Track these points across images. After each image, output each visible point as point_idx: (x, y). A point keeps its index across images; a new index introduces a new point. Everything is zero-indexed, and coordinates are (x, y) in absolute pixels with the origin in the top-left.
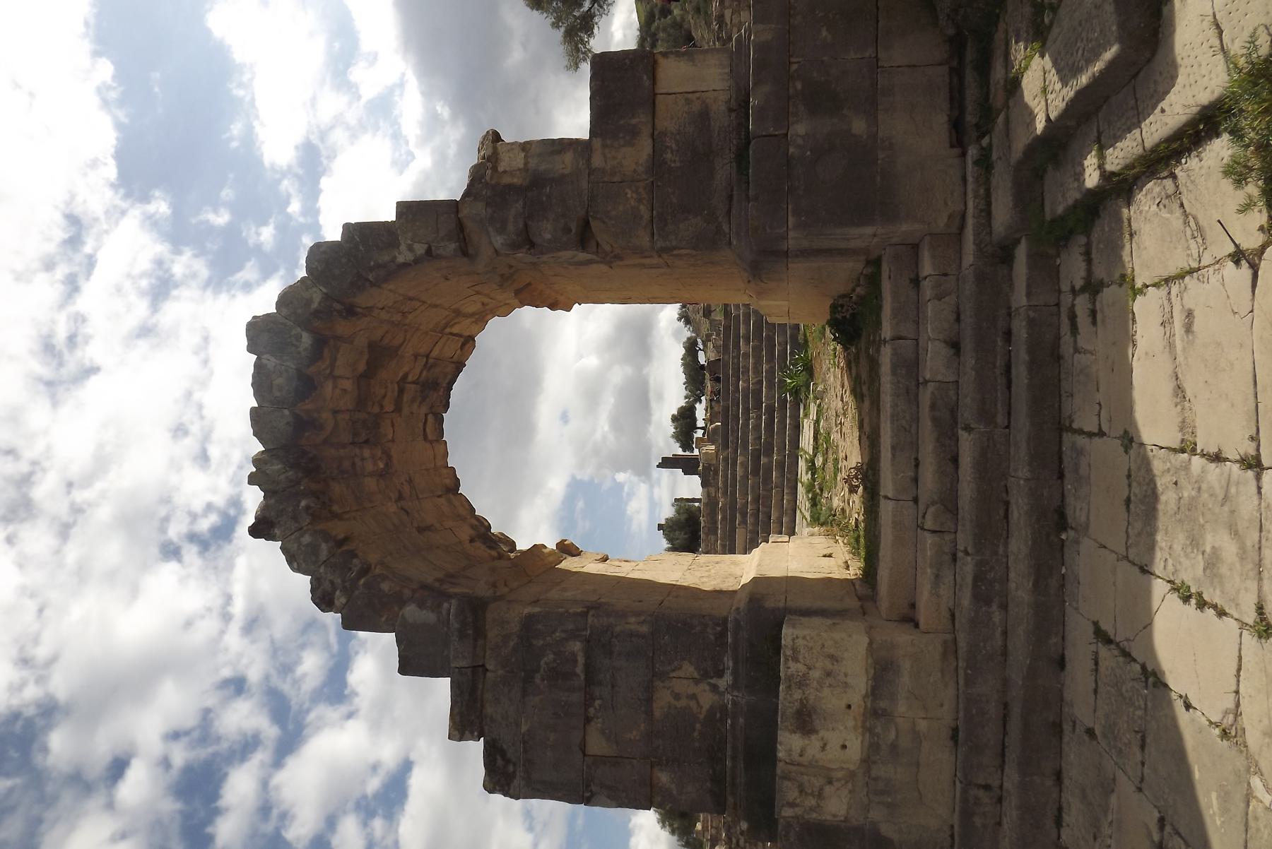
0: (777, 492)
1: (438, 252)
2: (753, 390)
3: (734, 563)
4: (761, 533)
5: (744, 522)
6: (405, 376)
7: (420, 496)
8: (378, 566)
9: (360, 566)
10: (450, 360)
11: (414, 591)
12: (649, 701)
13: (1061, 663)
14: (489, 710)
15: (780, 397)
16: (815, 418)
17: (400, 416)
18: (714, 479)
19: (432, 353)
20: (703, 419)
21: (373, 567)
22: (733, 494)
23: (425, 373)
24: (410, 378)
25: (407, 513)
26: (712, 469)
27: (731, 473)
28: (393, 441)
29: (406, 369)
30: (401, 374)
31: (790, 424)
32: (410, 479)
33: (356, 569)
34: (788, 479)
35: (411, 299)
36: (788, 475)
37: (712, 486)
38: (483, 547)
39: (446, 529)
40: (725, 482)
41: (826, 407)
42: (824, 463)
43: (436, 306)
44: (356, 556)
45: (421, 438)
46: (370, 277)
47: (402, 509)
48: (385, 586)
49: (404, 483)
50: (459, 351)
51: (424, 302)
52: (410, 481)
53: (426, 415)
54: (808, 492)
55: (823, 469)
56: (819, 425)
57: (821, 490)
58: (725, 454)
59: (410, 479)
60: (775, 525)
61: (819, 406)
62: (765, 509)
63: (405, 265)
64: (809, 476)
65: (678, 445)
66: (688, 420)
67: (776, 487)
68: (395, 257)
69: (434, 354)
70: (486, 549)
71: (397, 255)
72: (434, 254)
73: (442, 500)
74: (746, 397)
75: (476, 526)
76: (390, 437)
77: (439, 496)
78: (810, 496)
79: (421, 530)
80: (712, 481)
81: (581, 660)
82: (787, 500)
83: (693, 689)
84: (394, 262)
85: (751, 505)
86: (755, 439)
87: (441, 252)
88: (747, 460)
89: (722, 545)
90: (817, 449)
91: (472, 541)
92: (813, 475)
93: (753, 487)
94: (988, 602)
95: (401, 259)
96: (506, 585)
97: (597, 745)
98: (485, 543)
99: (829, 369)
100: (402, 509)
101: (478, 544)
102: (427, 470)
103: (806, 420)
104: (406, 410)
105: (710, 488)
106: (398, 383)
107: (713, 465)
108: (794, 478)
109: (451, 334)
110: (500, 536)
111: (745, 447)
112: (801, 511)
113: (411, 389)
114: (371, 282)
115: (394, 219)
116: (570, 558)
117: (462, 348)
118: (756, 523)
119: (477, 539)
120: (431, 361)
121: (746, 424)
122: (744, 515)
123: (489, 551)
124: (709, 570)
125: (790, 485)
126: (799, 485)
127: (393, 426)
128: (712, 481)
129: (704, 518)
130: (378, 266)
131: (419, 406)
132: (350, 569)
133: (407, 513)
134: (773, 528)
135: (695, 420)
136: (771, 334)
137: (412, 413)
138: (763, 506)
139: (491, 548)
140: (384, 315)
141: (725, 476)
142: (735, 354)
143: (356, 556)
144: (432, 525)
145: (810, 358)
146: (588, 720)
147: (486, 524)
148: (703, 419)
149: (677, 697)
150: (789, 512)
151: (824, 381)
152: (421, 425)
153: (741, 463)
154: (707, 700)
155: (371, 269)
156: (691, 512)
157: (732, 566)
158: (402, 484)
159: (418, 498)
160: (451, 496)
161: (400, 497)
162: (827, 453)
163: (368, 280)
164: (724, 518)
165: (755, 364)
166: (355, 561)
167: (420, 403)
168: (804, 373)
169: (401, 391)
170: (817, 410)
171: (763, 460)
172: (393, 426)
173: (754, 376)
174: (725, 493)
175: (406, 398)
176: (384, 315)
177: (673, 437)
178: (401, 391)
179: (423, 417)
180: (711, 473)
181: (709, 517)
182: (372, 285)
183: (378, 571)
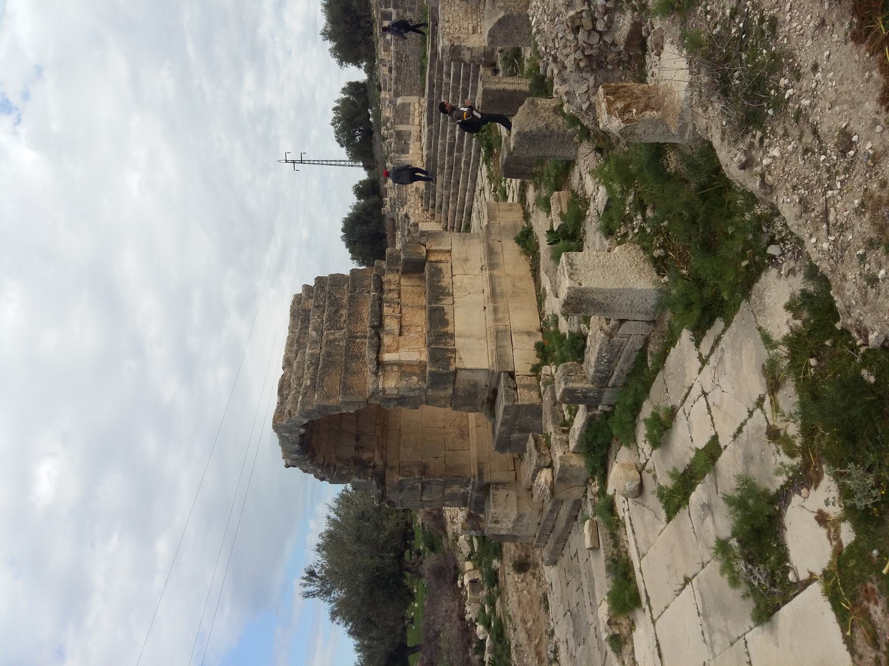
11: (354, 469)
12: (444, 492)
13: (570, 533)
14: (387, 495)
18: (402, 3)
37: (400, 8)
48: (344, 472)
80: (400, 5)
81: (420, 487)
82: (471, 186)
83: (458, 489)
86: (451, 137)
93: (448, 162)
94: (553, 512)
97: (425, 498)
105: (399, 9)
108: (475, 175)
111: (444, 135)
122: (442, 169)
128: (400, 5)
136: (466, 87)
146: (422, 495)
149: (453, 490)
154: (462, 490)
165: (453, 96)
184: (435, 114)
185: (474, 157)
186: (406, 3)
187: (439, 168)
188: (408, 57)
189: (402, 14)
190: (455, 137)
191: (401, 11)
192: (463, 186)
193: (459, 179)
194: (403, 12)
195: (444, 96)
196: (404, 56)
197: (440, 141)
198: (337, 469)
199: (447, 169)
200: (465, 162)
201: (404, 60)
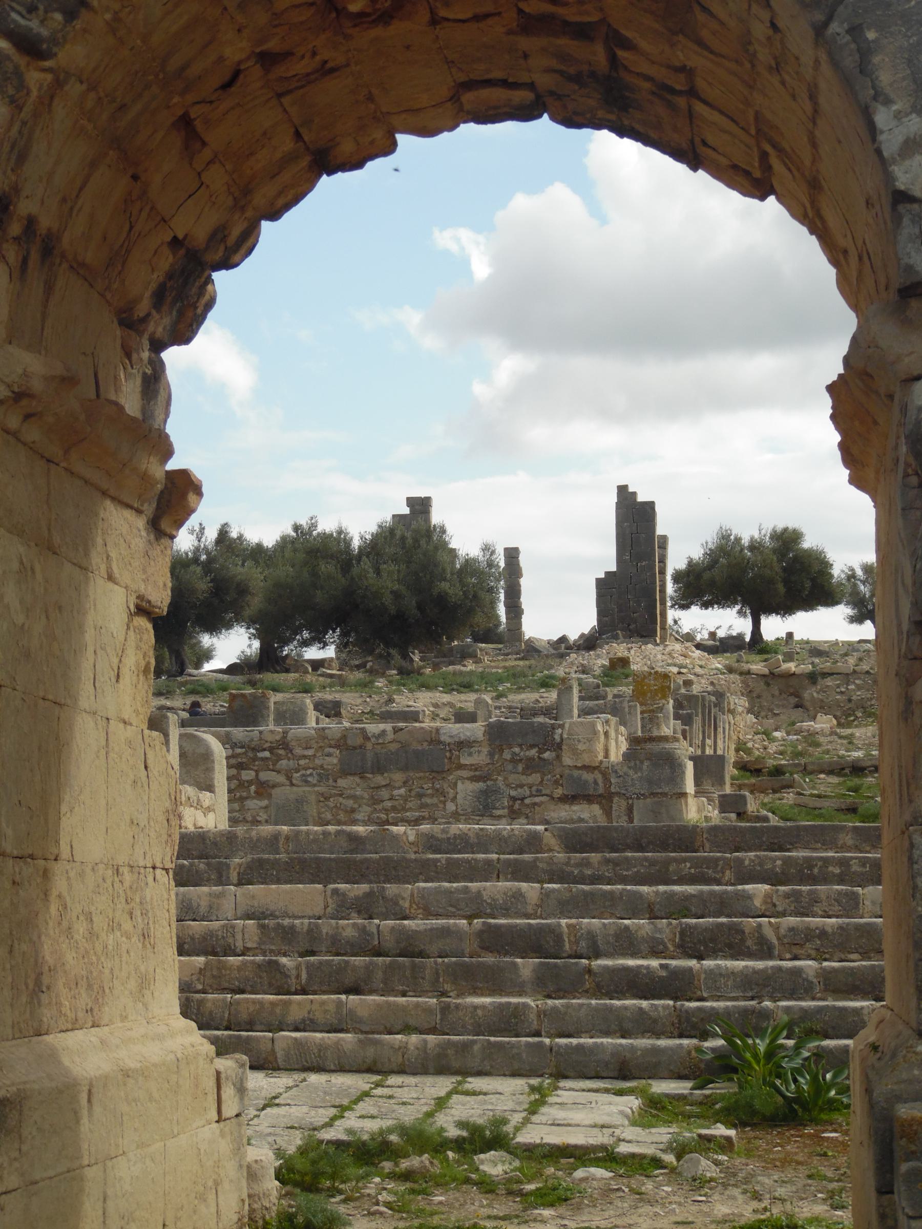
0: (428, 1010)
1: (906, 221)
2: (737, 930)
3: (145, 983)
4: (309, 966)
5: (344, 907)
6: (627, 45)
7: (286, 100)
8: (49, 77)
9: (45, 32)
10: (697, 140)
15: (713, 1016)
16: (623, 1149)
17: (510, 32)
18: (514, 761)
19: (698, 103)
20: (790, 635)
21: (47, 64)
22: (427, 871)
23: (646, 85)
24: (621, 53)
25: (226, 86)
26: (547, 755)
27: (489, 862)
28: (435, 21)
29: (643, 44)
30: (628, 34)
31: (632, 1048)
32: (333, 70)
33: (33, 24)
34: (465, 1047)
35: (813, 97)
36: (476, 1047)
37: (491, 754)
38: (157, 278)
39: (199, 174)
40: (463, 843)
41: (649, 1186)
42: (487, 1186)
43: (814, 145)
44: (70, 16)
45: (462, 78)
46: (835, 27)
47: (236, 74)
49: (318, 58)
50: (724, 161)
51: (815, 123)
52: (326, 71)
53: (531, 86)
54: (402, 1130)
55: (467, 1181)
56: (597, 1162)
57: (407, 1176)
58: (550, 839)
59: (333, 70)
60: (331, 1008)
61: (656, 1163)
62: (380, 975)
63: (873, 130)
64: (453, 1132)
65: (697, 553)
66: (781, 588)
67: (445, 1009)
68: (888, 102)
69: (699, 107)
70: (153, 286)
71: (895, 107)
72: (901, 208)
73: (287, 144)
74: (722, 905)
75: (224, 239)
76: (443, 13)
77: (298, 135)
78: (394, 1138)
79: (185, 123)
80: (507, 755)
82: (403, 1048)
84: (875, 98)
85: (447, 859)
86: (591, 936)
87: (908, 229)
88: (530, 910)
89: (276, 837)
90: (529, 1158)
91: (175, 243)
92: (458, 1144)
93: (445, 932)
95: (882, 117)
96: (27, 417)
98: (170, 276)
99: (757, 1196)
100: (236, 74)
101: (167, 261)
102: (370, 98)
103: (633, 1103)
104: (525, 43)
105: (485, 750)
106: (603, 20)
107: (558, 757)
109: (764, 156)
110: (203, 301)
111: (567, 907)
112: (367, 1094)
113: (597, 54)
114: (826, 24)
115: (615, 569)
116: (141, 523)
117: (735, 167)
118: (338, 946)
119: (182, 252)
120: (682, 102)
121: (636, 907)
123: (148, 294)
124: (113, 926)
125: (450, 1052)
126: (442, 1085)
127: (477, 18)
128: (507, 755)
129: (390, 736)
130: (865, 53)
131: (549, 70)
132: (32, 9)
133: (226, 86)
134: (323, 1003)
135: (786, 608)
137: (526, 56)
138: (390, 967)
139: (159, 297)
140: (760, 30)
141: (483, 843)
142: (855, 868)
143: (70, 16)
144: (204, 144)
145: (824, 1116)
147: (236, 258)
148: (790, 635)
150: (370, 1052)
151: (729, 1179)
152: (497, 74)
153: (518, 896)
155: (855, 31)
156: (470, 611)
157: (132, 984)
158: (314, 54)
159: (280, 95)
160: (305, 162)
161: (268, 59)
162: (510, 1193)
163: (830, 19)
164: (354, 838)
165: (823, 933)
166: (58, 16)
167: (561, 73)
168: (780, 1099)
169: (582, 32)
170: (642, 1157)
171: (526, 966)
172: (477, 18)
173: (782, 931)
174: (432, 844)
175: (564, 42)
176: (760, 30)
177: (725, 536)
178: (582, 32)
179: (525, 78)
180: (533, 752)
181: (394, 747)
182: (820, 30)
183: (36, 79)
184: (652, 863)
185: (580, 1047)
186: (512, 778)
187: (369, 895)
188: (259, 795)
189: (465, 760)
190: (597, 956)
191: (479, 757)
192: (363, 1013)
193: (371, 992)
194: (475, 768)
195: (787, 896)
196: (264, 776)
197: (530, 889)
198: (20, 60)
199: (402, 933)
200: (518, 1012)
201: (248, 775)
